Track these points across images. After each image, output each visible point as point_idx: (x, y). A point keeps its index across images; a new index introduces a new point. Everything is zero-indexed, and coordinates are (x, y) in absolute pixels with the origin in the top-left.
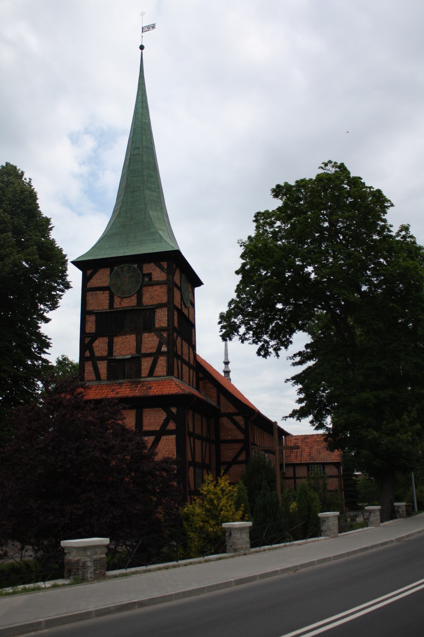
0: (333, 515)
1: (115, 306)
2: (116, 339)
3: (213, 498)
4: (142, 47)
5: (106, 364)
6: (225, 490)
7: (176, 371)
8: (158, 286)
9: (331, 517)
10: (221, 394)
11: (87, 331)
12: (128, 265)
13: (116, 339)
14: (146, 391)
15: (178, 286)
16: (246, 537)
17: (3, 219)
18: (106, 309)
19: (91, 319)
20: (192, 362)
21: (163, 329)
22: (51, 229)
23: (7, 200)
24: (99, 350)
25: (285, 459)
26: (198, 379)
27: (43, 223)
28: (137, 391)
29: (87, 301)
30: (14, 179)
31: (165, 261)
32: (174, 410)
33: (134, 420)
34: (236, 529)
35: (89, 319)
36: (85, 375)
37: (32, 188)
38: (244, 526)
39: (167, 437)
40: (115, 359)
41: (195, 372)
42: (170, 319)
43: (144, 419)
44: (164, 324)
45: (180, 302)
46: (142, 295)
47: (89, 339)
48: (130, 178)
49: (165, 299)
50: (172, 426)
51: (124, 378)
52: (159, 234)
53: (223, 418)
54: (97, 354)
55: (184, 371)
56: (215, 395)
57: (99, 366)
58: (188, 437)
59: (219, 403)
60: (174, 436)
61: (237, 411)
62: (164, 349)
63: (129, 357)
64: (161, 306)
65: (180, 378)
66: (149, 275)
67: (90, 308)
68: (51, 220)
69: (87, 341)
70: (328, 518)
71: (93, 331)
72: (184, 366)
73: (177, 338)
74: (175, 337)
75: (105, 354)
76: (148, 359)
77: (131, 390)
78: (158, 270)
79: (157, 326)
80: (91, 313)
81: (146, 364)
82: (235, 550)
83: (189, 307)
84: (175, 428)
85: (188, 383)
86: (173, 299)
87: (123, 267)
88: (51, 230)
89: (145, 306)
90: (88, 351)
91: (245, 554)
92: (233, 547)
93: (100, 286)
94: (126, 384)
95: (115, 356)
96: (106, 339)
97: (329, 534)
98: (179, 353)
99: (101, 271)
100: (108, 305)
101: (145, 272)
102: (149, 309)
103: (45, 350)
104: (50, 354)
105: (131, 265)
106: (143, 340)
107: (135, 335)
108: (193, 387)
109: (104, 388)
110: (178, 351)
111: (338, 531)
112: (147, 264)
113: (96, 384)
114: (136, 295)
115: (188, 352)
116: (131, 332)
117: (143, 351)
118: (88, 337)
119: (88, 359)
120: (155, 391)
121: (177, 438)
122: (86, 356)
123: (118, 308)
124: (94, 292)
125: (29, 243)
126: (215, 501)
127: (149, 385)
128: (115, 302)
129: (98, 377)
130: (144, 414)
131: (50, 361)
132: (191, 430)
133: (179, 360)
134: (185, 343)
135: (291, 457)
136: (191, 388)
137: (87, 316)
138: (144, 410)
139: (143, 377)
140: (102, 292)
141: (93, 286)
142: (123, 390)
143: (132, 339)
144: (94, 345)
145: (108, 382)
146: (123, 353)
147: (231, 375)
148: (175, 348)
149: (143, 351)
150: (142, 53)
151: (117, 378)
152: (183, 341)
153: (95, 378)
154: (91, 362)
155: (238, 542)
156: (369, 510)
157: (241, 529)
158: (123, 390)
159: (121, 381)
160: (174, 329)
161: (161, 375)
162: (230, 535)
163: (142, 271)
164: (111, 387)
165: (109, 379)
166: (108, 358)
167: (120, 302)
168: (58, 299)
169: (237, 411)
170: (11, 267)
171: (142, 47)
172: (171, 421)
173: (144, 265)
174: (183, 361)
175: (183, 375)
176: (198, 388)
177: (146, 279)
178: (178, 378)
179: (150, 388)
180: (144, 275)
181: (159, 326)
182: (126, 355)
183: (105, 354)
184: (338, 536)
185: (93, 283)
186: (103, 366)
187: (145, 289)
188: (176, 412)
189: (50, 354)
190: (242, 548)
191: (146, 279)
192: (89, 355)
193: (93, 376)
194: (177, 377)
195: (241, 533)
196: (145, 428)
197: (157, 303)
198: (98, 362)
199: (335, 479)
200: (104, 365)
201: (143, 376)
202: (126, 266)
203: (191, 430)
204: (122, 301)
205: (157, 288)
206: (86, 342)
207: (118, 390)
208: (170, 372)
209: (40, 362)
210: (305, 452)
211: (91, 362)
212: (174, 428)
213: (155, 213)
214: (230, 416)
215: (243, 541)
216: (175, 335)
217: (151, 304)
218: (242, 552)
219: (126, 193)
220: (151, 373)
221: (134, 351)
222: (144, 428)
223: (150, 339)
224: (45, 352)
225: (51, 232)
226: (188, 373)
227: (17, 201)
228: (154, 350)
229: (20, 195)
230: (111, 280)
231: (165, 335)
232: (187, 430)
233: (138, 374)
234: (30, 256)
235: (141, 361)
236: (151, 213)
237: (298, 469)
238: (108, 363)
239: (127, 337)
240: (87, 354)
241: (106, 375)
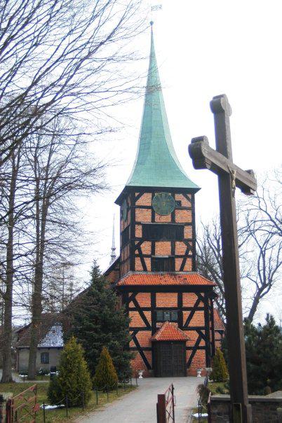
2: (156, 244)
13: (156, 244)
32: (203, 294)
50: (201, 305)
54: (144, 253)
57: (146, 262)
62: (190, 253)
64: (188, 224)
75: (150, 253)
79: (185, 237)
80: (139, 223)
81: (178, 262)
116: (168, 240)
119: (137, 256)
129: (145, 269)
143: (168, 244)
165: (152, 271)
171: (152, 23)
183: (150, 253)
186: (148, 262)
193: (141, 268)
202: (163, 194)
205: (185, 211)
220: (182, 269)
233: (173, 268)
240: (137, 252)
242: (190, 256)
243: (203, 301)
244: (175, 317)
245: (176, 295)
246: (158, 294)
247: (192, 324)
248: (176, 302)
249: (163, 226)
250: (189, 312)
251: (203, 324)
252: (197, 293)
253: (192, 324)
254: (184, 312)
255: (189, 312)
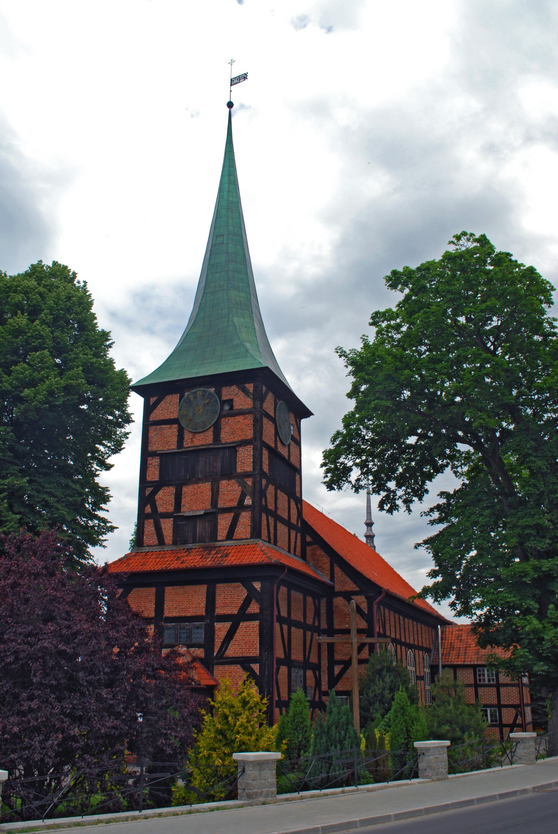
0: (437, 745)
1: (185, 445)
2: (185, 489)
3: (228, 713)
4: (230, 105)
5: (172, 523)
6: (249, 702)
7: (264, 532)
8: (241, 417)
9: (434, 748)
10: (335, 565)
11: (149, 479)
12: (202, 389)
14: (221, 559)
15: (271, 416)
16: (270, 776)
17: (39, 332)
18: (173, 449)
19: (154, 462)
20: (294, 520)
21: (247, 475)
22: (110, 346)
23: (48, 309)
24: (163, 503)
25: (442, 659)
26: (304, 545)
27: (96, 337)
28: (209, 560)
29: (150, 439)
30: (59, 282)
31: (251, 383)
32: (257, 585)
33: (205, 599)
34: (252, 762)
35: (151, 462)
36: (145, 537)
37: (88, 294)
38: (267, 758)
39: (248, 623)
40: (183, 516)
41: (299, 534)
42: (257, 461)
43: (217, 598)
44: (249, 468)
45: (273, 437)
46: (221, 428)
47: (151, 489)
48: (210, 275)
49: (250, 434)
50: (254, 608)
51: (194, 542)
52: (244, 346)
53: (339, 598)
54: (160, 510)
55: (278, 533)
56: (328, 566)
57: (163, 526)
58: (277, 626)
59: (332, 578)
60: (257, 623)
61: (357, 589)
62: (248, 501)
63: (202, 512)
64: (244, 443)
65: (272, 541)
66: (230, 402)
67: (152, 448)
68: (111, 334)
69: (148, 491)
70: (428, 749)
71: (157, 479)
72: (279, 525)
73: (267, 486)
74: (263, 486)
75: (171, 509)
76: (226, 515)
77: (201, 558)
78: (241, 394)
79: (239, 470)
80: (154, 454)
81: (224, 522)
82: (249, 796)
83: (289, 445)
84: (258, 611)
85: (286, 548)
86: (262, 434)
87: (195, 393)
88: (111, 347)
89: (224, 444)
90: (149, 506)
91: (264, 804)
92: (246, 791)
93: (166, 418)
94: (196, 550)
95: (184, 512)
96: (172, 490)
97: (430, 775)
98: (271, 507)
99: (168, 398)
100: (176, 443)
101: (224, 398)
102: (228, 448)
103: (103, 506)
104: (108, 511)
105: (206, 389)
106: (221, 490)
107: (210, 483)
108: (295, 554)
109: (168, 555)
110: (268, 504)
111: (447, 770)
112: (228, 387)
113: (158, 550)
114: (212, 429)
115: (287, 506)
116: (205, 479)
117: (220, 505)
118: (149, 487)
119: (148, 516)
120: (232, 560)
121: (260, 625)
122: (146, 512)
123: (188, 447)
124: (158, 427)
125: (75, 363)
126: (230, 718)
127: (226, 551)
128: (186, 439)
129: (161, 541)
130: (218, 591)
131: (109, 520)
132: (284, 614)
133: (270, 517)
134: (283, 494)
135: (451, 655)
136: (292, 556)
137: (149, 458)
138: (218, 585)
139: (219, 541)
140: (169, 426)
141: (158, 418)
142: (191, 558)
144: (157, 497)
145: (174, 548)
146: (194, 508)
147: (376, 541)
148: (263, 500)
149: (220, 505)
150: (230, 113)
151: (185, 542)
152: (279, 492)
153: (157, 542)
154: (152, 521)
155: (254, 783)
156: (516, 738)
157: (260, 764)
158: (191, 558)
159: (190, 546)
160: (263, 474)
161: (244, 537)
162: (244, 771)
163: (220, 396)
164: (177, 553)
165: (175, 543)
166: (175, 515)
167: (192, 439)
168: (122, 439)
169: (357, 589)
170: (45, 394)
172: (253, 601)
173: (223, 388)
174: (278, 518)
175: (278, 538)
176: (303, 556)
177: (227, 408)
178: (269, 542)
179: (227, 555)
180: (223, 402)
181: (241, 471)
182: (198, 510)
184: (448, 778)
185: (157, 415)
186: (167, 526)
187: (224, 421)
188: (261, 588)
189: (108, 511)
190: (261, 793)
191: (227, 408)
192: (150, 510)
194: (267, 540)
195: (260, 770)
196: (219, 611)
197: (240, 439)
198: (162, 521)
199: (514, 688)
200: (170, 525)
201: (219, 538)
202: (199, 391)
203: (284, 614)
204: (194, 438)
205: (240, 418)
206: (147, 493)
207: (186, 558)
208: (256, 533)
209: (96, 522)
210: (471, 648)
211: (152, 521)
212: (257, 611)
213: (242, 320)
214: (348, 596)
215: (263, 781)
216: (264, 482)
217: (231, 441)
218: (262, 799)
219: (205, 295)
220: (230, 536)
221: (208, 506)
222: (217, 610)
223: (229, 488)
224: (102, 509)
225: (110, 349)
226: (287, 535)
227: (61, 309)
228: (235, 504)
229: (65, 302)
230: (180, 410)
231: (249, 482)
232: (276, 613)
233: (213, 536)
234: (73, 380)
235: (217, 519)
236: (235, 319)
237: (459, 673)
238: (174, 521)
239: (199, 485)
240: (148, 509)
241: (172, 538)
242: (248, 507)
243: (260, 601)
244: (199, 636)
245: (153, 590)
246: (168, 589)
247: (232, 651)
248: (203, 604)
249: (197, 452)
250: (228, 625)
251: (255, 652)
252: (247, 583)
253: (232, 651)
254: (217, 625)
255: (228, 625)
